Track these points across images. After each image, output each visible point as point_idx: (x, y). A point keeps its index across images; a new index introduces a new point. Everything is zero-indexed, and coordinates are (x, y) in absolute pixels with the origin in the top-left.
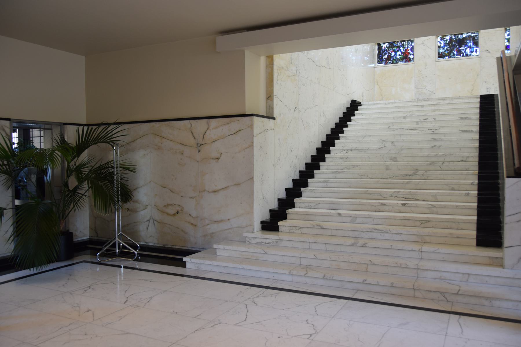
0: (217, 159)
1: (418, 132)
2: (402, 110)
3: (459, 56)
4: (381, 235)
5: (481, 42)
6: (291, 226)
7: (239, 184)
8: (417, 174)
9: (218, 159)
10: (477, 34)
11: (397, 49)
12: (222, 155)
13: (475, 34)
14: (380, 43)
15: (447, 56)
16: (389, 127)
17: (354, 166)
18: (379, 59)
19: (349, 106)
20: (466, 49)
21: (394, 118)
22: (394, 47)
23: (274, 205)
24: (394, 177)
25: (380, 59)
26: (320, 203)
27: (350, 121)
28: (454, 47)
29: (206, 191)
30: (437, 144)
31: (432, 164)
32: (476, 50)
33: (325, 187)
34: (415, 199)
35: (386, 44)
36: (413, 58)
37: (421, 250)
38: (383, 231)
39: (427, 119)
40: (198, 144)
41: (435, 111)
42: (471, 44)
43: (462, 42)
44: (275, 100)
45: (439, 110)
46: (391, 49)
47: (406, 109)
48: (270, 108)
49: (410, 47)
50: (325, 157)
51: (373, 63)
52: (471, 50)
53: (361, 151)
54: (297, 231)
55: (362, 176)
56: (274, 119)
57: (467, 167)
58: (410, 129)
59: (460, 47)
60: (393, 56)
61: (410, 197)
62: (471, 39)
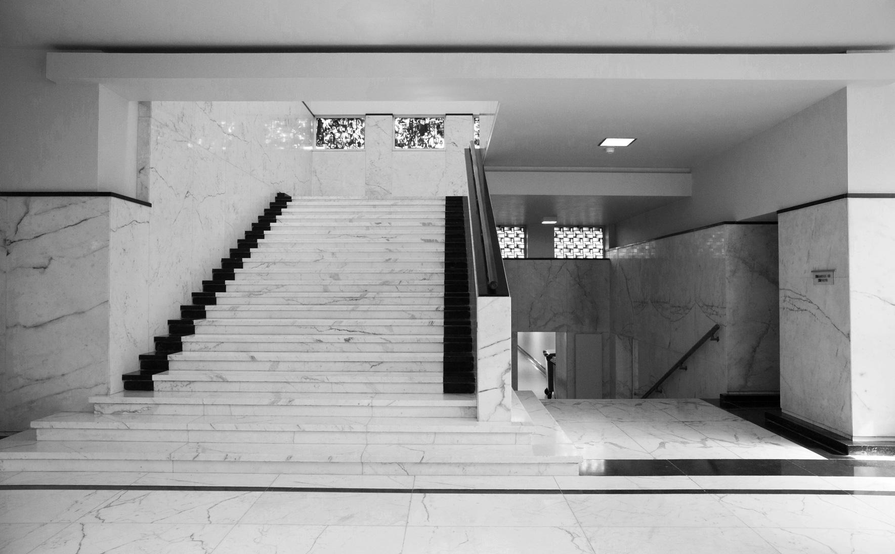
0: (43, 269)
1: (369, 241)
2: (347, 210)
3: (421, 147)
4: (315, 386)
5: (446, 132)
6: (174, 381)
7: (83, 312)
8: (366, 298)
9: (45, 268)
10: (442, 121)
11: (344, 129)
12: (52, 261)
13: (440, 121)
14: (320, 119)
15: (406, 145)
16: (329, 232)
17: (277, 286)
19: (274, 201)
20: (429, 139)
21: (336, 220)
22: (339, 125)
23: (149, 348)
24: (335, 302)
25: (320, 140)
26: (223, 343)
27: (275, 221)
28: (415, 135)
29: (20, 325)
30: (393, 256)
31: (385, 283)
32: (441, 141)
33: (233, 317)
34: (363, 332)
35: (329, 121)
36: (364, 144)
37: (370, 405)
38: (317, 380)
39: (381, 223)
40: (5, 240)
41: (390, 213)
42: (434, 132)
43: (424, 129)
44: (152, 176)
45: (396, 213)
46: (335, 128)
47: (353, 210)
48: (144, 187)
49: (361, 128)
50: (235, 272)
51: (310, 144)
52: (435, 140)
53: (289, 265)
54: (184, 389)
55: (289, 301)
56: (149, 205)
57: (430, 288)
58: (358, 237)
59: (423, 134)
61: (356, 330)
62: (436, 127)
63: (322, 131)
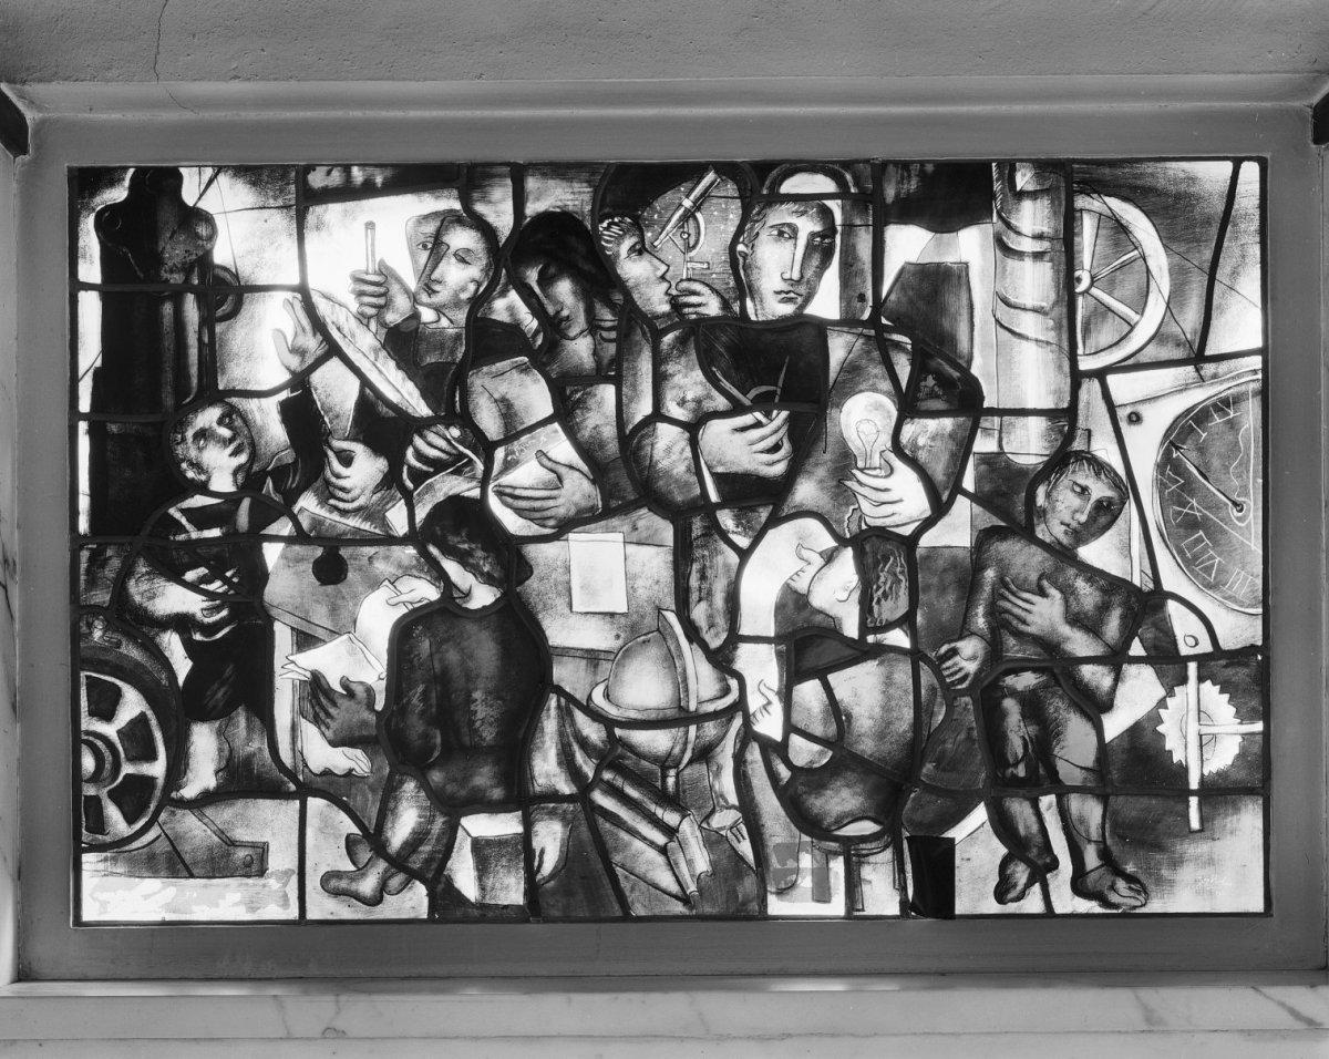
14: (158, 185)
18: (132, 704)
60: (597, 637)
63: (221, 468)
